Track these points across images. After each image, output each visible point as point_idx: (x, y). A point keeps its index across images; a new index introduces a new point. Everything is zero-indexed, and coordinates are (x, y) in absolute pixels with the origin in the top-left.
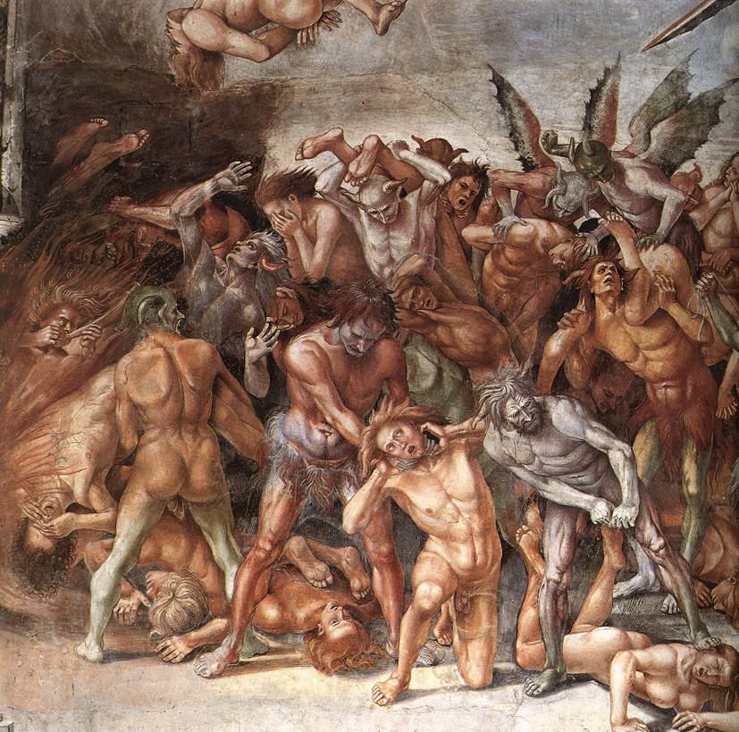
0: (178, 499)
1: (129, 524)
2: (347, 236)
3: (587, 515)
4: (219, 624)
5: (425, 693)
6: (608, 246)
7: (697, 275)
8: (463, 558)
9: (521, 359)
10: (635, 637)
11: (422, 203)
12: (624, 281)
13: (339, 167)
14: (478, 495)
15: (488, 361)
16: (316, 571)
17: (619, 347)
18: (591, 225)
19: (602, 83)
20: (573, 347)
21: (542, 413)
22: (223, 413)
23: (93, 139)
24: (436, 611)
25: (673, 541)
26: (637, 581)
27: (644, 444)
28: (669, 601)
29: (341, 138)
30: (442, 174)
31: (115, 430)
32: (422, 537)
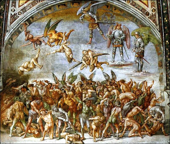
0: (19, 119)
1: (14, 122)
2: (37, 91)
3: (63, 120)
4: (24, 132)
5: (46, 140)
6: (65, 92)
7: (75, 95)
8: (50, 125)
9: (56, 104)
10: (68, 133)
11: (45, 87)
12: (67, 96)
13: (36, 83)
14: (51, 118)
15: (52, 104)
16: (34, 127)
17: (66, 102)
18: (63, 89)
19: (64, 74)
20: (61, 103)
21: (58, 110)
22: (24, 110)
23: (10, 81)
24: (47, 131)
25: (72, 123)
26: (68, 127)
27: (69, 113)
28: (72, 130)
29: (36, 80)
30: (47, 84)
31: (13, 112)
32: (45, 123)
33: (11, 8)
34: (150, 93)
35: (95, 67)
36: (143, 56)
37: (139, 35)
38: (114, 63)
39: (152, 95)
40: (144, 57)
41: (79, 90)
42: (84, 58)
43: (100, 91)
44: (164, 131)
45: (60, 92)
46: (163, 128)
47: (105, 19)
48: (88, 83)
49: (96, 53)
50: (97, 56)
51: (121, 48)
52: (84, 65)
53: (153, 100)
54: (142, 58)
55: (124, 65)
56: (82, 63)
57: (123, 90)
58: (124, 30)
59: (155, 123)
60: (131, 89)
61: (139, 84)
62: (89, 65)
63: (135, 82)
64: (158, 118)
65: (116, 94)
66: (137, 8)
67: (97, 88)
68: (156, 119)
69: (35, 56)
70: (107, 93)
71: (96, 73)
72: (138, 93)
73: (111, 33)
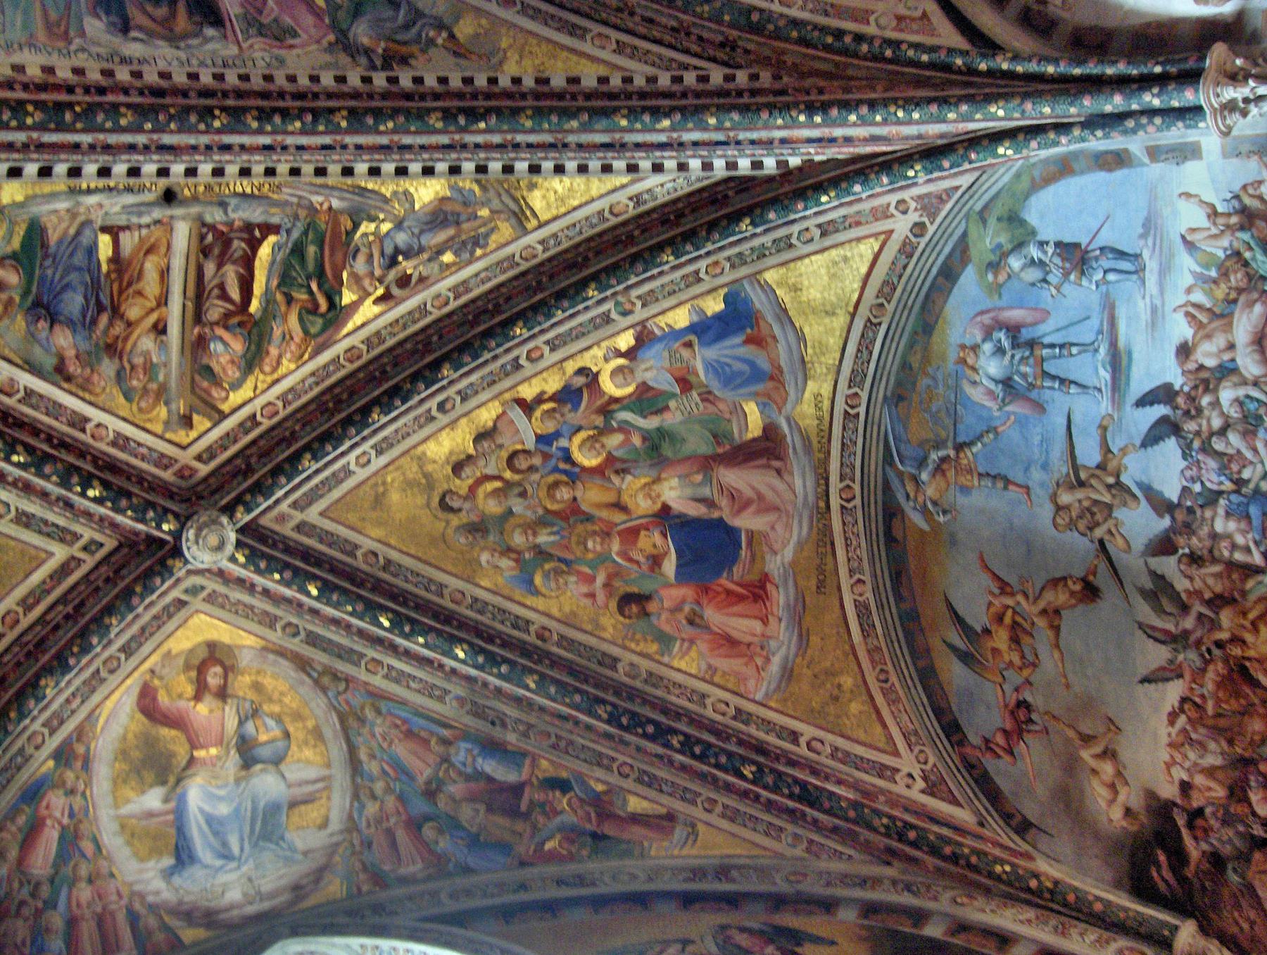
2: (1210, 772)
6: (1219, 644)
7: (1235, 600)
11: (1195, 731)
12: (1237, 640)
18: (1209, 651)
33: (899, 789)
34: (1237, 212)
35: (1118, 484)
36: (1076, 246)
37: (994, 266)
38: (1107, 392)
39: (1247, 201)
40: (1084, 241)
41: (1215, 575)
42: (1082, 525)
43: (1223, 469)
45: (1220, 666)
47: (943, 414)
48: (1187, 526)
49: (1064, 470)
50: (1075, 468)
51: (1045, 352)
52: (1110, 532)
54: (1087, 252)
55: (1113, 344)
56: (1101, 542)
57: (1221, 351)
58: (979, 339)
60: (1217, 310)
61: (1198, 269)
62: (1109, 507)
63: (1189, 291)
65: (1241, 392)
66: (900, 277)
67: (1208, 485)
69: (1068, 741)
70: (1234, 438)
71: (1145, 479)
72: (1239, 275)
73: (990, 393)
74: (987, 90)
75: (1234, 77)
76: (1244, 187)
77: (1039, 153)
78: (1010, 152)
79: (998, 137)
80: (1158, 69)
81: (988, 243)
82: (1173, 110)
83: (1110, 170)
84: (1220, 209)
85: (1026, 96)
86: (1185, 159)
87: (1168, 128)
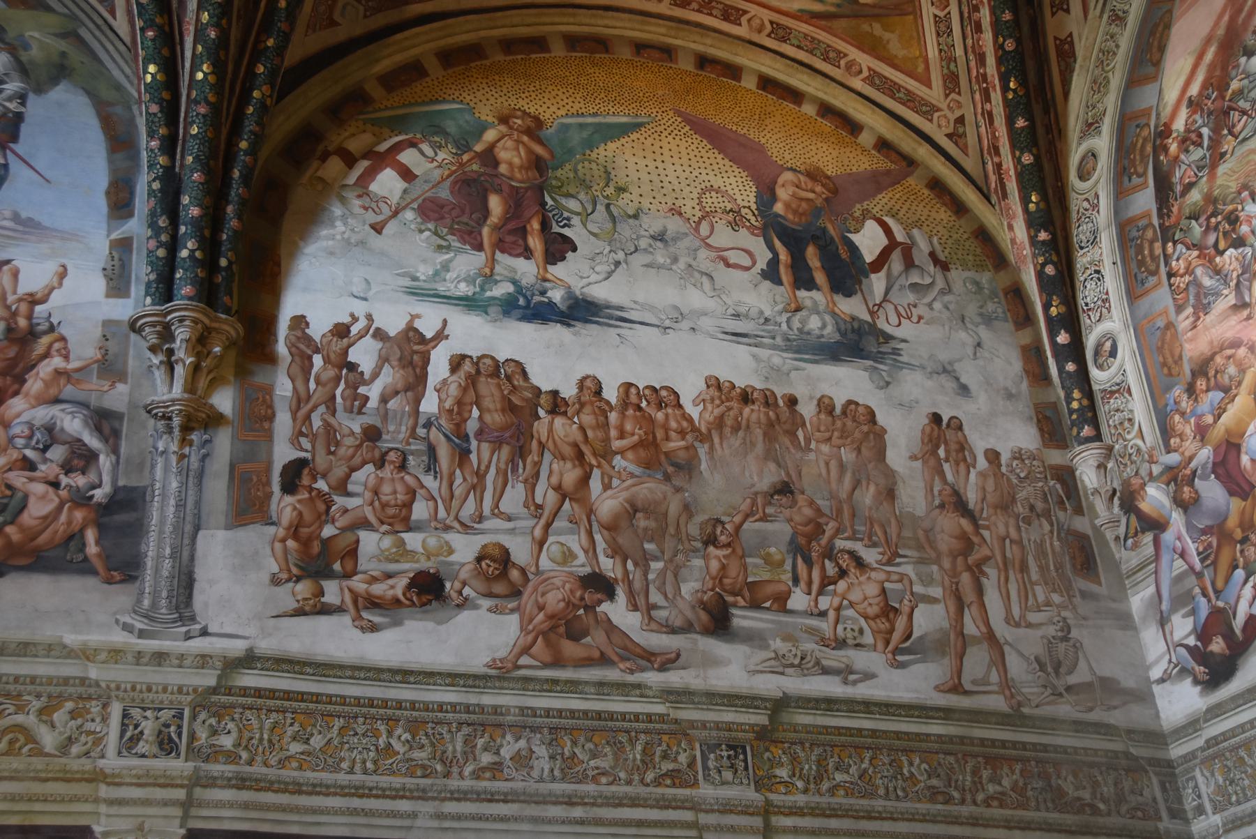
36: (15, 138)
39: (45, 340)
40: (18, 147)
44: (99, 555)
46: (90, 535)
53: (46, 369)
59: (43, 497)
64: (68, 469)
68: (51, 478)
74: (230, 67)
75: (201, 342)
76: (63, 339)
77: (142, 116)
78: (149, 78)
79: (170, 67)
80: (223, 262)
81: (33, 34)
82: (172, 271)
83: (108, 193)
84: (38, 308)
85: (215, 109)
86: (109, 279)
87: (150, 263)
